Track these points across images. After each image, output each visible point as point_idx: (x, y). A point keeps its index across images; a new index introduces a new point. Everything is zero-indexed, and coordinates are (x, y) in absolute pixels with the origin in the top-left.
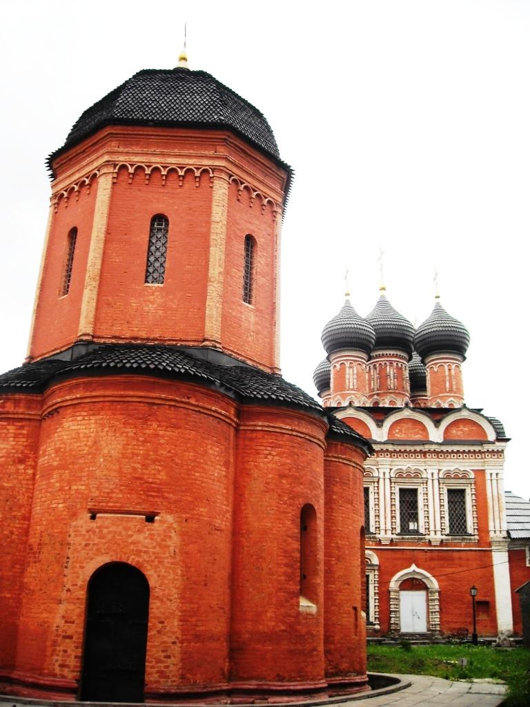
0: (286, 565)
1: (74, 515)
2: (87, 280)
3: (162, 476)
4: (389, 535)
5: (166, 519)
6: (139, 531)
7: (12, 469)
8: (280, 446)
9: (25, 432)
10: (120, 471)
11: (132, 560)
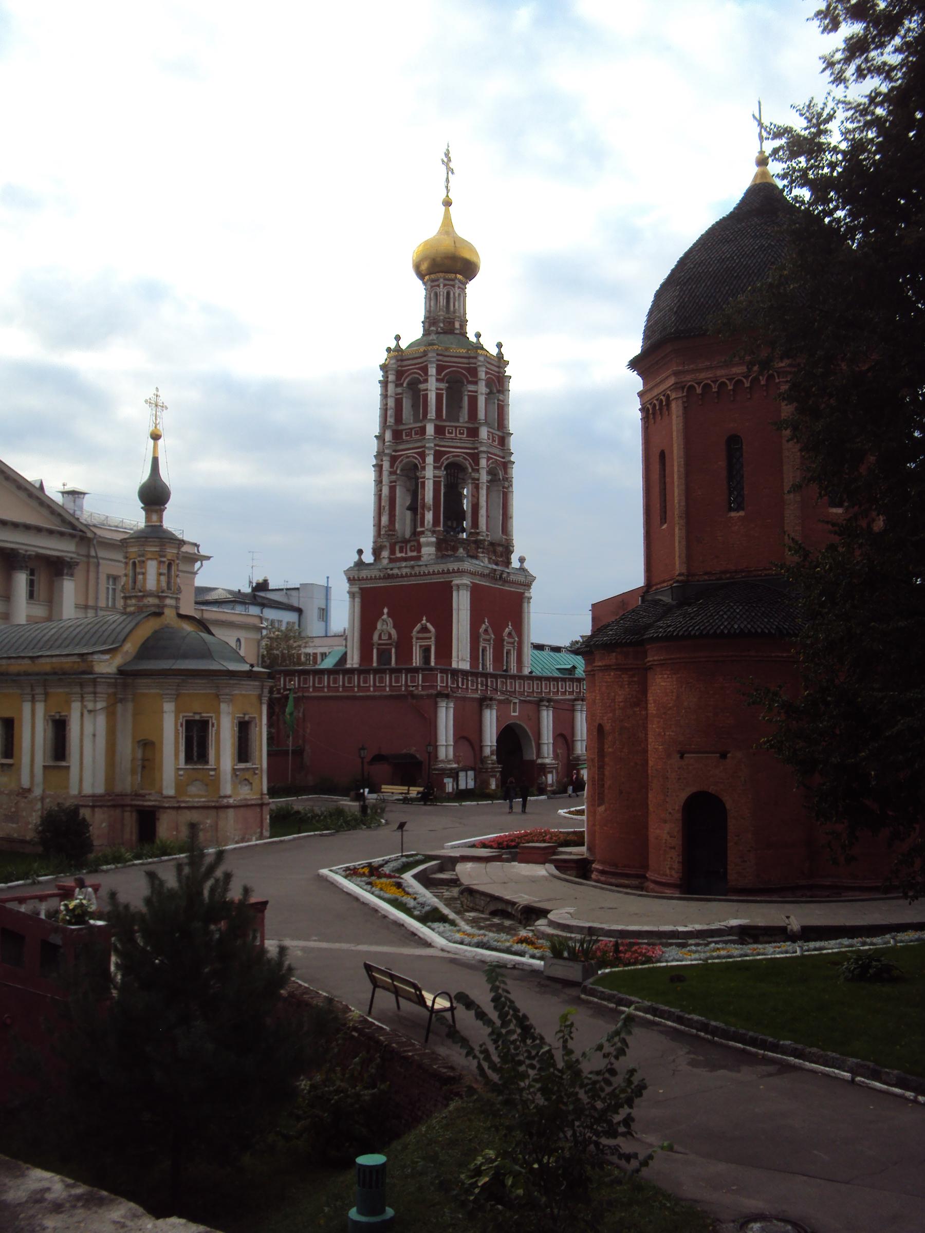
9: (636, 679)
11: (712, 789)
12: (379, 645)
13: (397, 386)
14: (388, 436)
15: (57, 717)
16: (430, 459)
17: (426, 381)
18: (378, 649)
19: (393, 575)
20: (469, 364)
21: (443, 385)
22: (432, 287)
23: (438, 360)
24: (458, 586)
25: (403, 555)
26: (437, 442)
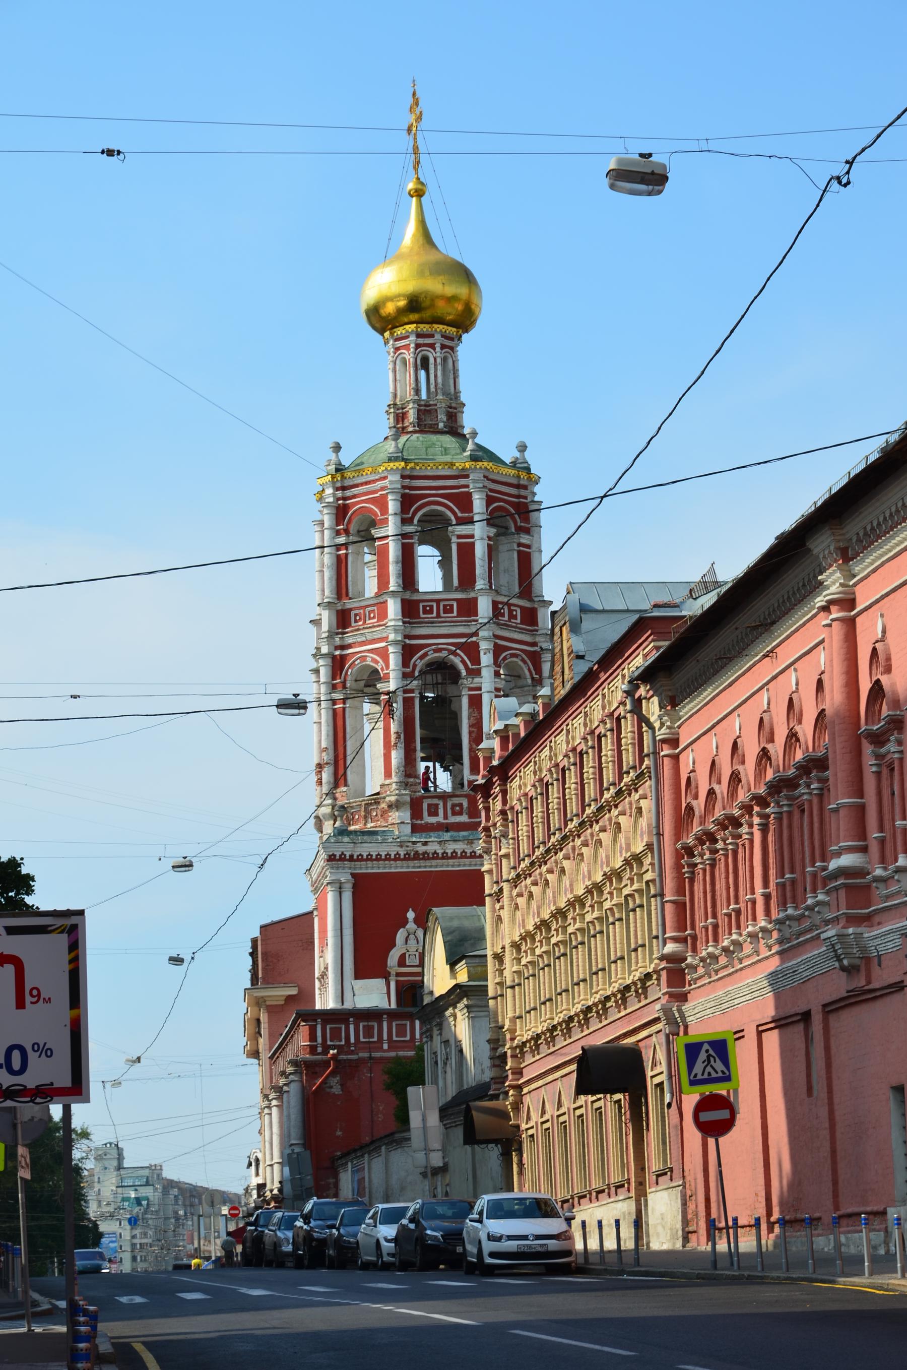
12: (398, 975)
13: (404, 522)
18: (397, 982)
19: (425, 853)
20: (518, 497)
22: (418, 346)
23: (491, 490)
25: (440, 819)
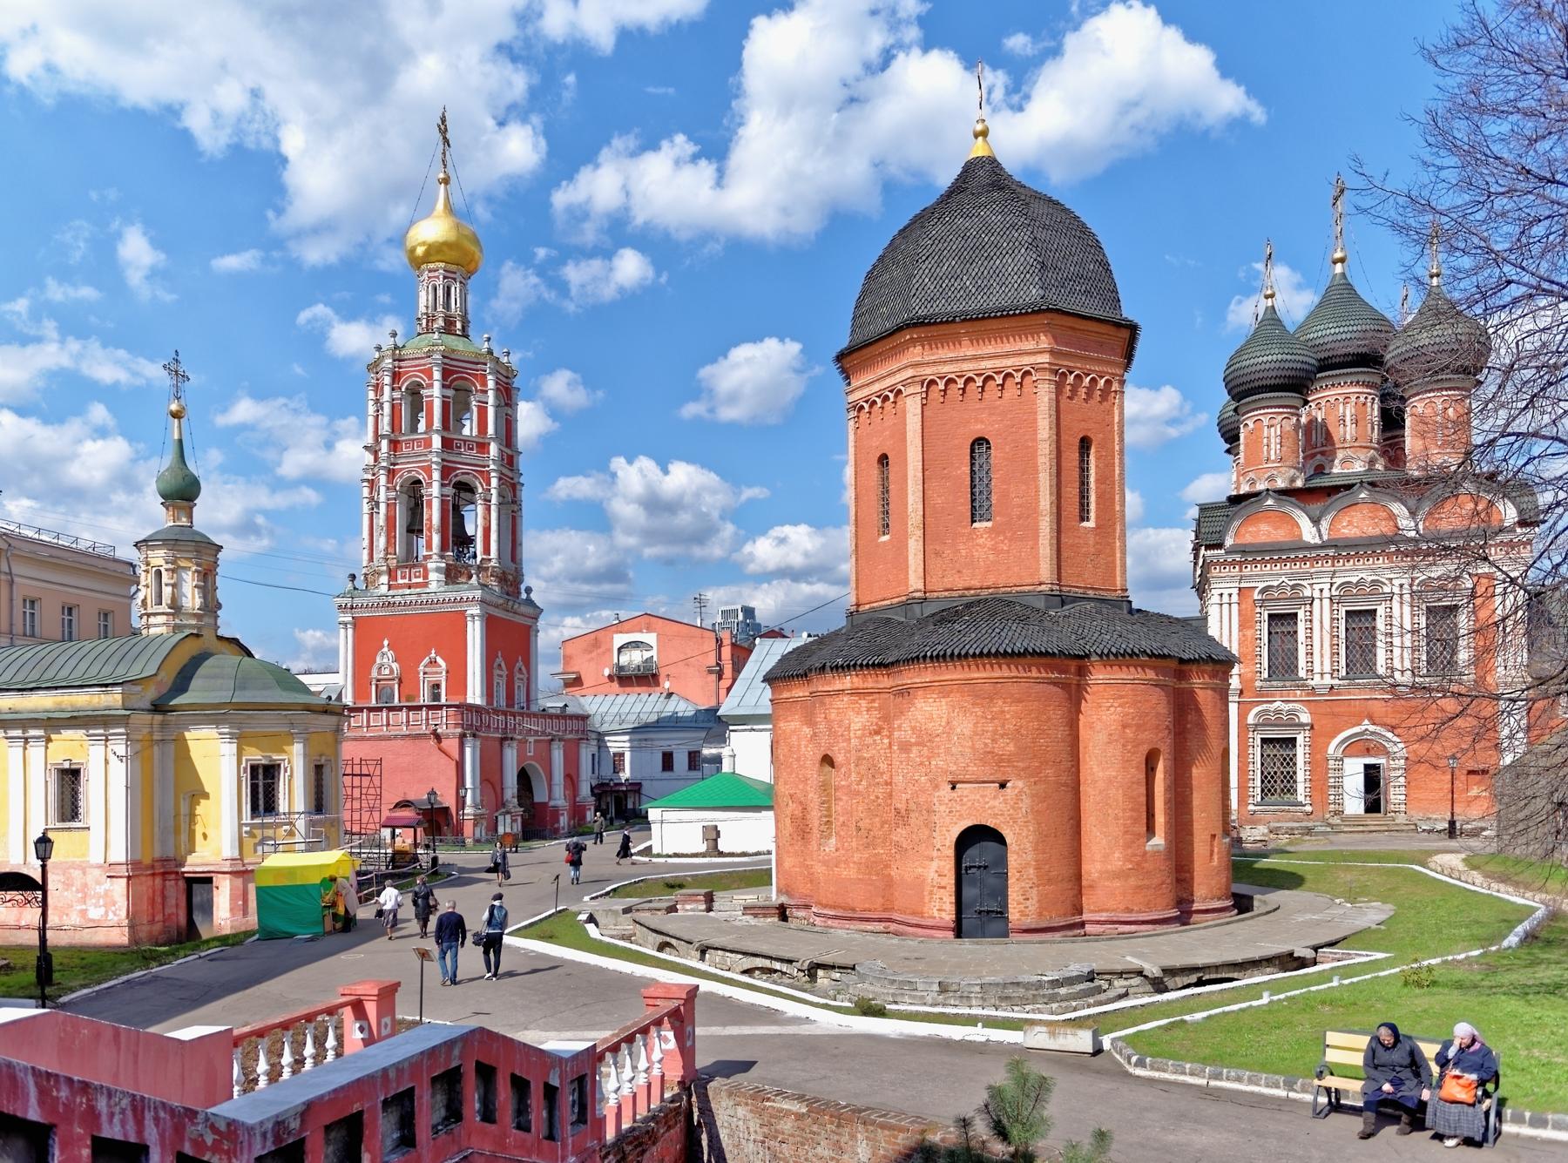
0: (1132, 810)
1: (937, 787)
2: (910, 528)
3: (1011, 748)
4: (1328, 680)
5: (1016, 785)
6: (995, 798)
7: (869, 740)
8: (1121, 697)
10: (973, 747)
11: (990, 823)
14: (384, 444)
15: (66, 765)
16: (436, 475)
17: (431, 386)
21: (450, 393)
24: (473, 616)
26: (446, 456)
